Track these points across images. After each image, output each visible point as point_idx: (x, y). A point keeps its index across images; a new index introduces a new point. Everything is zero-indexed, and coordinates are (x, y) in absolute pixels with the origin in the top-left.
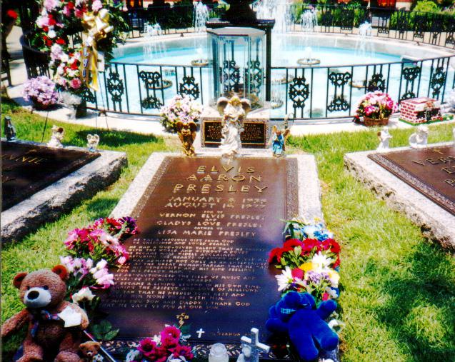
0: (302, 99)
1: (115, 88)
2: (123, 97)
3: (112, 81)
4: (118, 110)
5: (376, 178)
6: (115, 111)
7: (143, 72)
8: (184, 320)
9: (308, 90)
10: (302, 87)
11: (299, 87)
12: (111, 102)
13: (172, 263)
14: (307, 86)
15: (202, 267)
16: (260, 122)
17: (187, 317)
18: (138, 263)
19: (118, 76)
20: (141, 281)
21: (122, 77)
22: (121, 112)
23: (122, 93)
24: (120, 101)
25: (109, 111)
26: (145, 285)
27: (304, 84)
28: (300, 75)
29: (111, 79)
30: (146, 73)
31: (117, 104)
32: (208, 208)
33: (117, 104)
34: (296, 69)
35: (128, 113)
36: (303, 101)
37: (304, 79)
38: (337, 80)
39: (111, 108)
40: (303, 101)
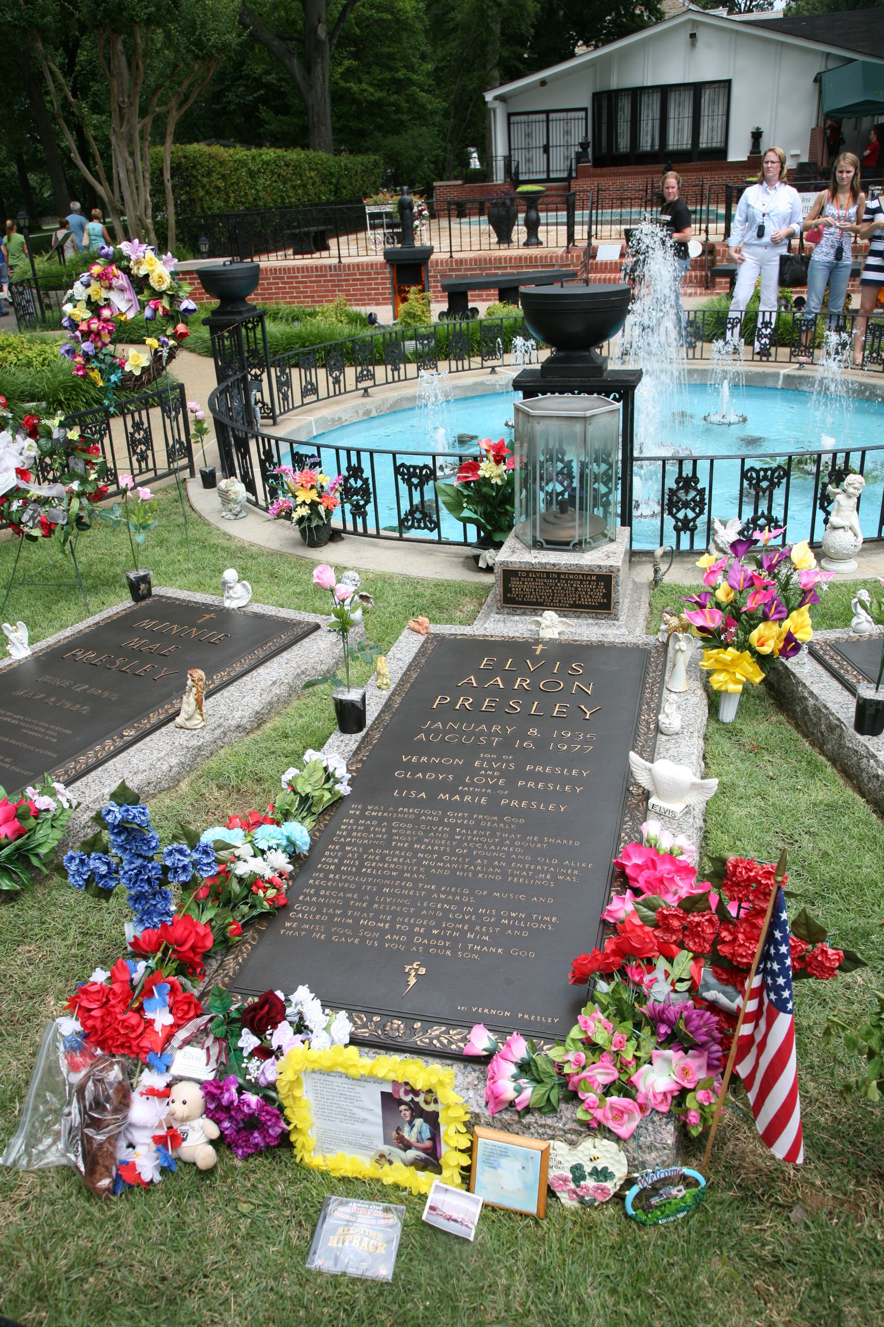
0: (691, 515)
1: (356, 492)
2: (370, 508)
3: (352, 481)
4: (360, 529)
5: (811, 693)
6: (355, 532)
7: (403, 465)
8: (417, 975)
9: (702, 499)
10: (692, 494)
11: (687, 493)
12: (349, 517)
13: (411, 858)
14: (701, 492)
15: (463, 870)
16: (604, 572)
17: (422, 971)
18: (353, 853)
19: (362, 471)
20: (353, 891)
21: (367, 474)
22: (365, 534)
23: (367, 502)
24: (364, 515)
25: (344, 530)
26: (360, 899)
27: (695, 489)
28: (687, 471)
29: (349, 477)
30: (408, 468)
31: (359, 521)
32: (488, 748)
33: (359, 521)
34: (681, 462)
35: (378, 536)
36: (694, 520)
37: (695, 478)
38: (759, 480)
39: (350, 527)
40: (694, 520)
